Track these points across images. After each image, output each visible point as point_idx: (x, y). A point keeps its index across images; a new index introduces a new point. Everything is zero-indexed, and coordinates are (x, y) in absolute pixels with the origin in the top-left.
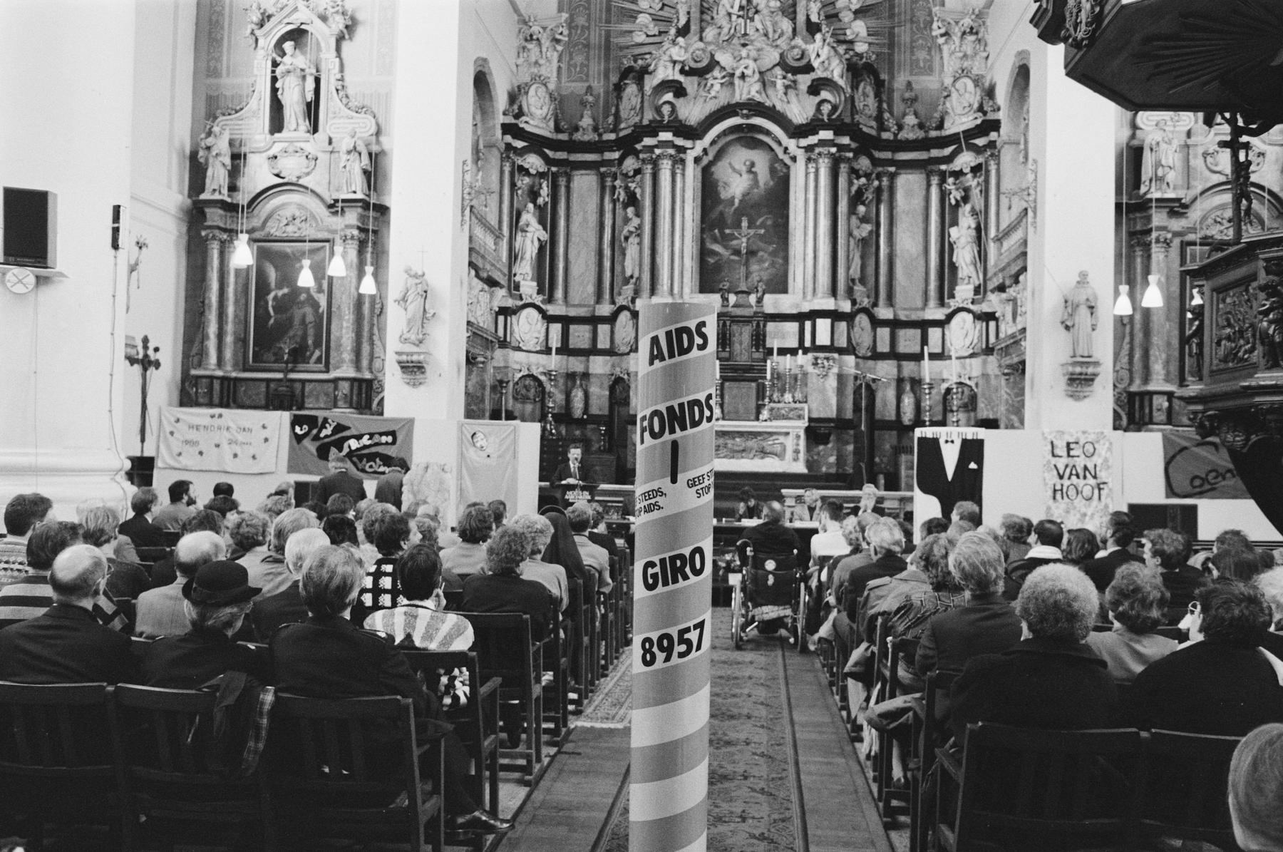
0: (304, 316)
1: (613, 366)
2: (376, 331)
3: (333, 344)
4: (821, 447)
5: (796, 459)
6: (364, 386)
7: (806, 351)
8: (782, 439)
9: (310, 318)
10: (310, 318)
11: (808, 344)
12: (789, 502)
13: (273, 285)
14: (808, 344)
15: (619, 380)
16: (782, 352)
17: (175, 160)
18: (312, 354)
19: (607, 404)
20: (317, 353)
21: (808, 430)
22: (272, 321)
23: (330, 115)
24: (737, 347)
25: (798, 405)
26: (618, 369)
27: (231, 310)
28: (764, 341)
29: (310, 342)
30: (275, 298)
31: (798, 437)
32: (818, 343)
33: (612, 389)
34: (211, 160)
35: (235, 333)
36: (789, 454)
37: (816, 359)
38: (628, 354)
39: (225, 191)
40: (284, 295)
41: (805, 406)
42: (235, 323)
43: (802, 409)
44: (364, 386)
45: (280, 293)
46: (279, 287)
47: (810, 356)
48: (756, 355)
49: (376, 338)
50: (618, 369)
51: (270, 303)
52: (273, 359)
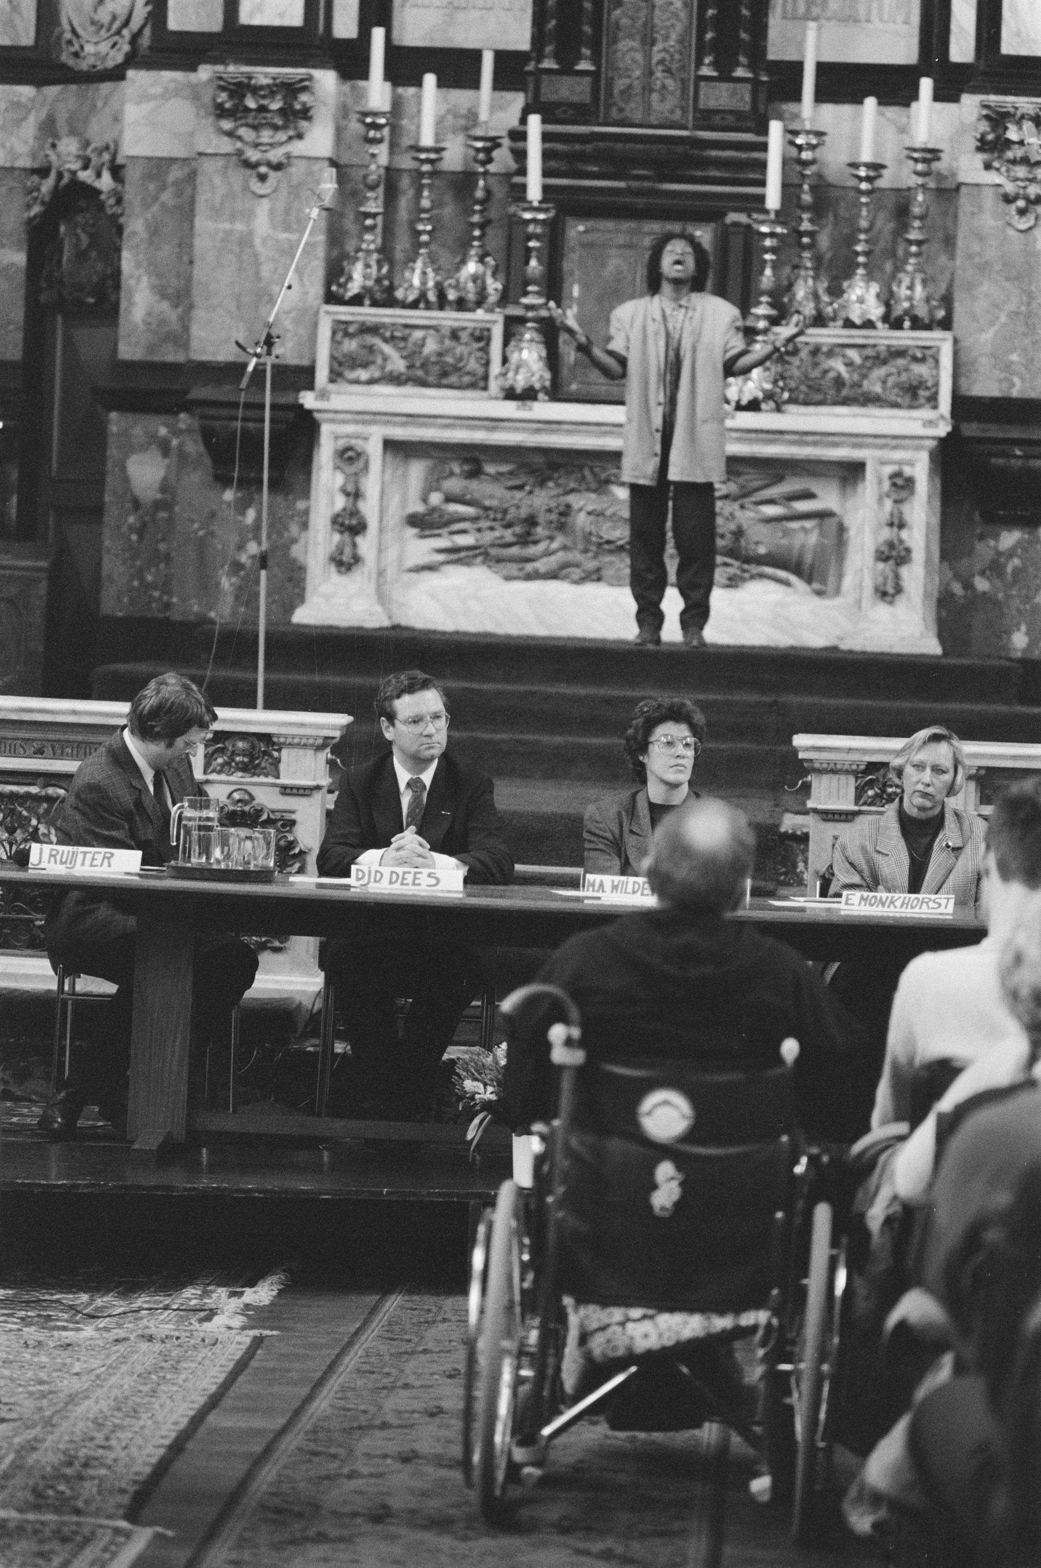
1: (49, 130)
4: (1009, 539)
5: (888, 593)
7: (952, 84)
8: (828, 498)
11: (962, 48)
12: (830, 793)
14: (962, 48)
15: (72, 199)
16: (844, 83)
19: (18, 314)
21: (948, 456)
24: (628, 51)
25: (906, 337)
26: (69, 146)
28: (759, 29)
31: (902, 484)
32: (1009, 46)
33: (40, 238)
36: (860, 564)
37: (998, 119)
38: (117, 74)
41: (942, 342)
43: (928, 356)
47: (970, 104)
48: (719, 97)
50: (69, 146)
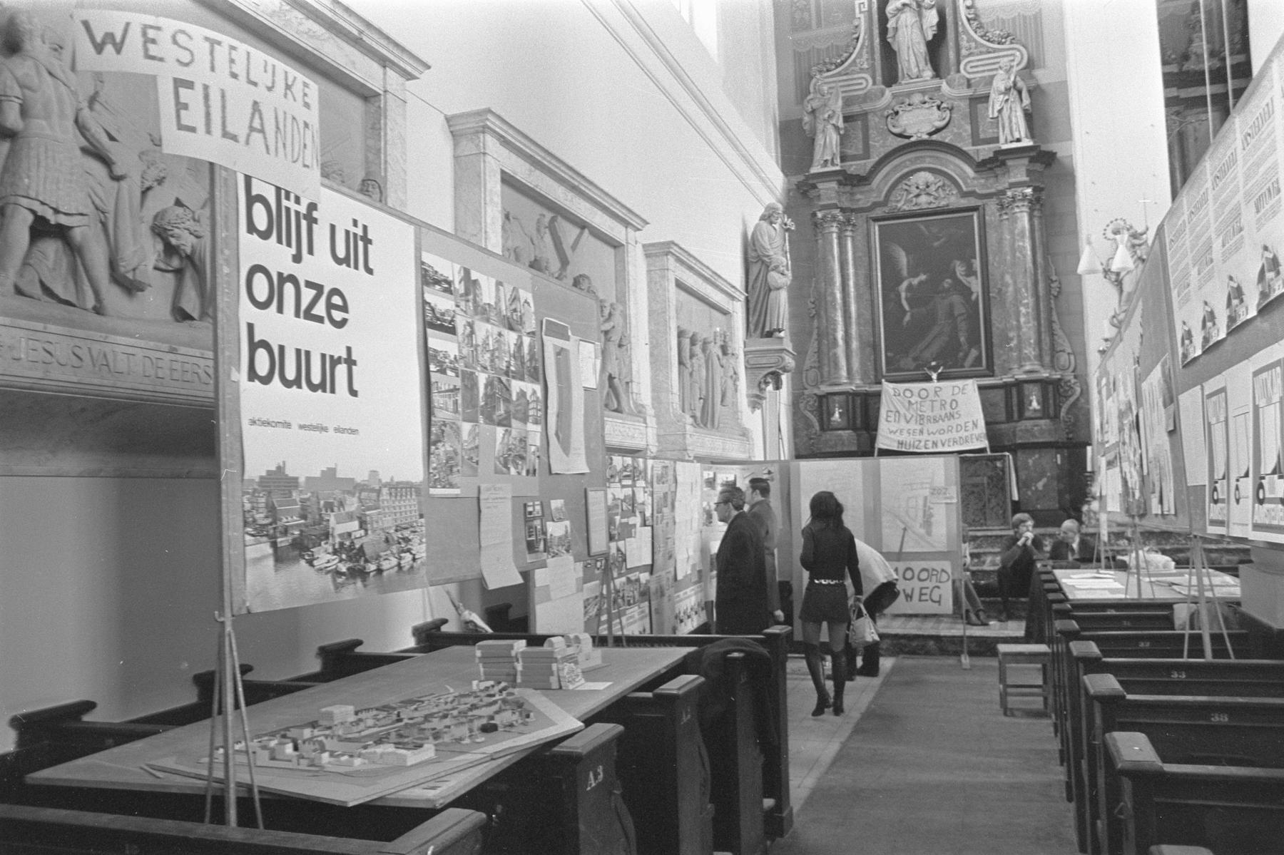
0: (951, 306)
2: (1055, 318)
3: (995, 340)
6: (1051, 388)
9: (959, 309)
10: (959, 309)
13: (905, 273)
17: (771, 129)
18: (966, 355)
20: (974, 353)
22: (907, 318)
23: (964, 52)
27: (853, 308)
29: (962, 339)
30: (910, 288)
34: (820, 127)
35: (860, 336)
39: (838, 161)
40: (921, 283)
42: (859, 324)
44: (1051, 388)
45: (915, 281)
46: (913, 274)
49: (1056, 326)
51: (903, 295)
52: (913, 365)
